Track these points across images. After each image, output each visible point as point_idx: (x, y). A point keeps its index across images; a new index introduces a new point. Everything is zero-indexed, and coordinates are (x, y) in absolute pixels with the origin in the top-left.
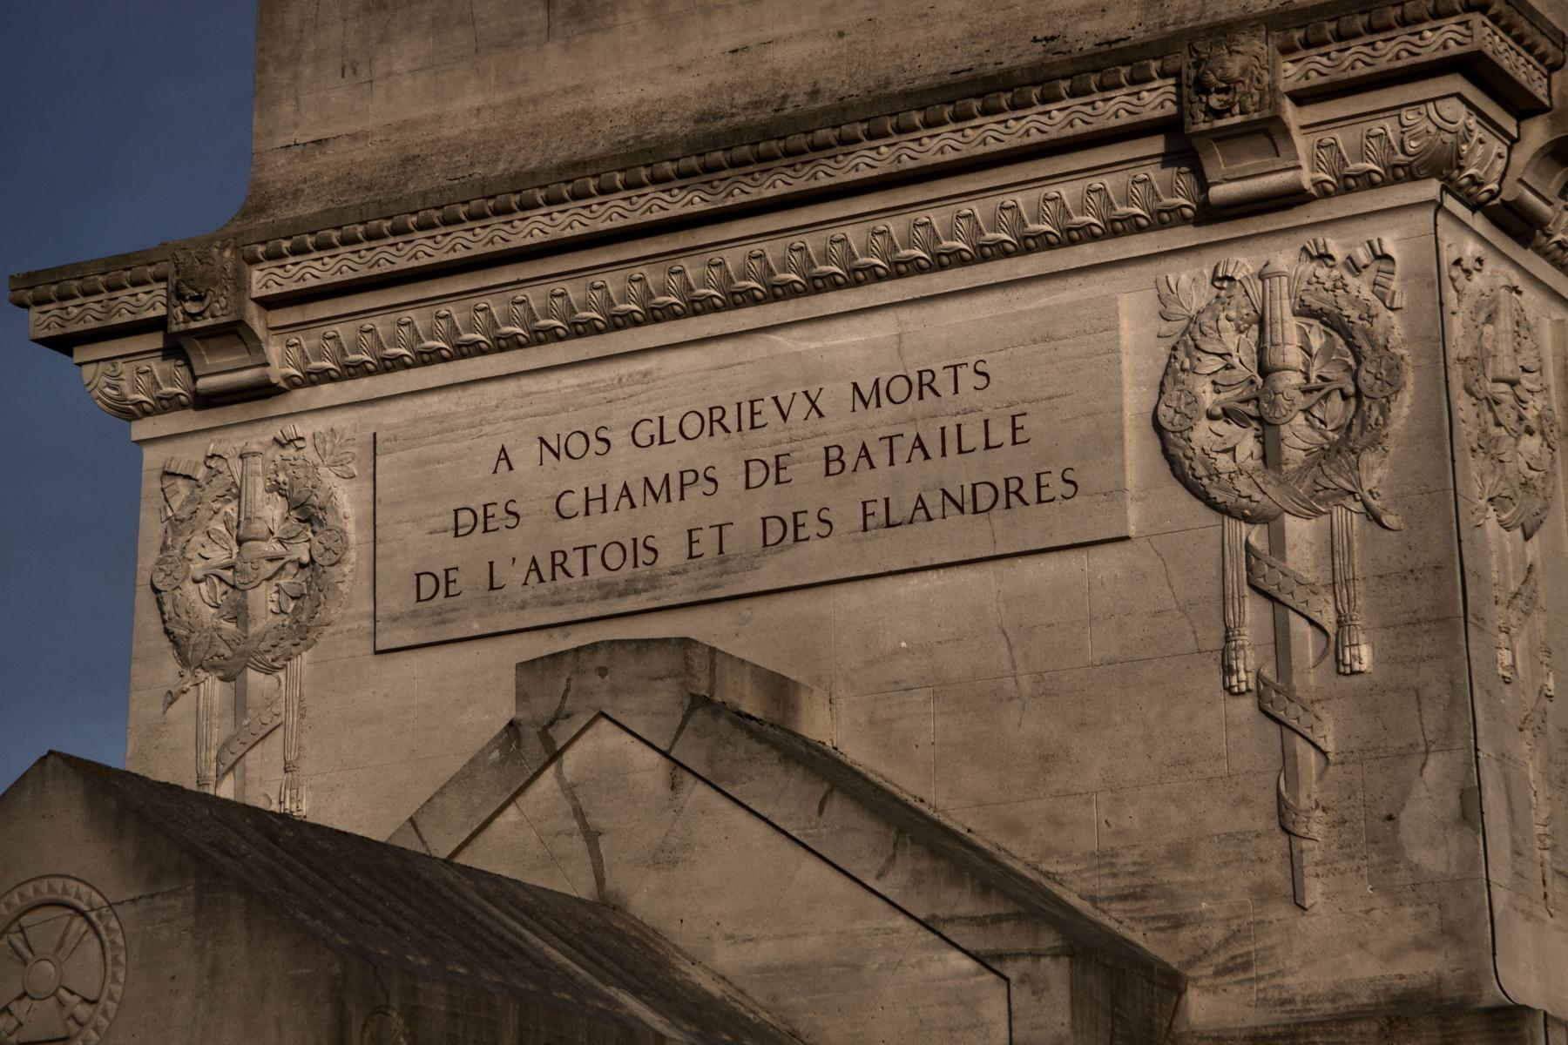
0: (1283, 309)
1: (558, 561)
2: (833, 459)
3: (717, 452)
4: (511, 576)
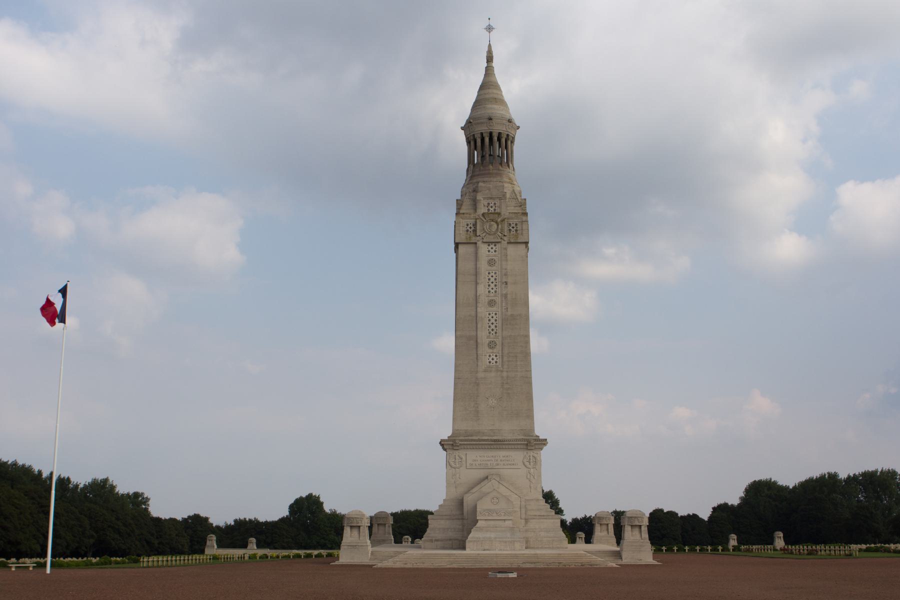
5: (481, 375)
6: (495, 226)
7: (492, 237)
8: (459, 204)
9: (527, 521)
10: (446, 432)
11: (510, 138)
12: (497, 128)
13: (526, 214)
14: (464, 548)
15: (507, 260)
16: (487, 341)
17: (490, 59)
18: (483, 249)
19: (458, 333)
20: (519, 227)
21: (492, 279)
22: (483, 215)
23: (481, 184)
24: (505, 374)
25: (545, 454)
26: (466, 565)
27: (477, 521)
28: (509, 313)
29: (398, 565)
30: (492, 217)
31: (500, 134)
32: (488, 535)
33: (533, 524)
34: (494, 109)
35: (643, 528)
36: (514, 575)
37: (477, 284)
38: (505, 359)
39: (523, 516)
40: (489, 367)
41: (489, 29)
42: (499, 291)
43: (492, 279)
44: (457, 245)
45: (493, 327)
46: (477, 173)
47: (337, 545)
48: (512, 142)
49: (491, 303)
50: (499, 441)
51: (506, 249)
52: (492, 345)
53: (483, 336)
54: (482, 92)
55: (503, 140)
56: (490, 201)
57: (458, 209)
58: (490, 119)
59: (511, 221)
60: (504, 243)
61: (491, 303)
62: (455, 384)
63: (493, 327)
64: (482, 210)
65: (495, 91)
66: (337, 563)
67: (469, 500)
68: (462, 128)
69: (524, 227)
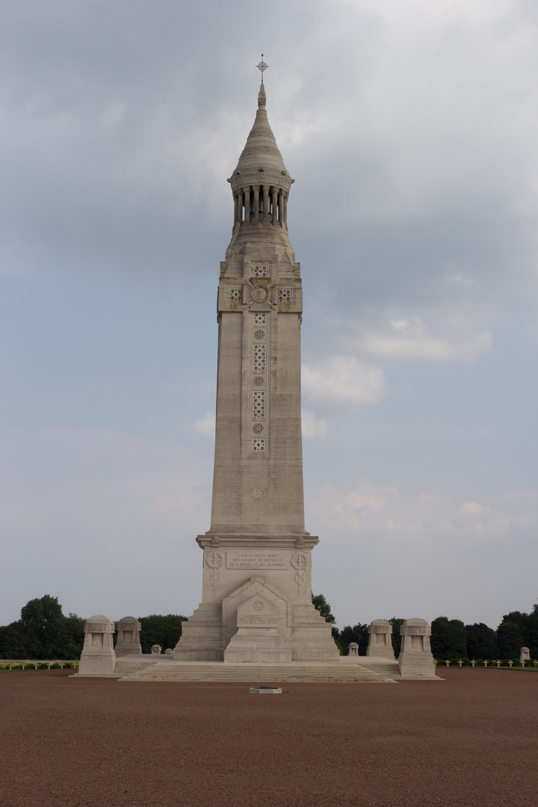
0: (300, 555)
1: (242, 564)
2: (266, 560)
3: (257, 558)
4: (239, 565)
5: (244, 462)
6: (264, 293)
7: (260, 305)
8: (224, 267)
9: (293, 629)
10: (204, 528)
11: (284, 193)
12: (268, 182)
13: (299, 280)
14: (222, 659)
15: (276, 333)
16: (253, 424)
17: (262, 102)
18: (250, 319)
19: (220, 415)
20: (291, 295)
21: (260, 354)
22: (251, 280)
23: (248, 245)
24: (272, 462)
25: (316, 553)
26: (224, 679)
27: (237, 629)
28: (279, 392)
29: (146, 678)
30: (260, 282)
31: (271, 188)
32: (249, 645)
33: (300, 633)
34: (266, 160)
35: (424, 638)
36: (279, 691)
37: (242, 358)
38: (273, 444)
39: (290, 624)
41: (262, 67)
42: (267, 367)
43: (260, 354)
44: (220, 314)
45: (259, 408)
46: (244, 232)
47: (78, 656)
48: (286, 198)
49: (258, 381)
50: (264, 538)
51: (275, 319)
52: (258, 429)
53: (249, 419)
54: (253, 139)
55: (275, 196)
56: (259, 265)
57: (223, 273)
58: (261, 171)
60: (274, 313)
61: (258, 381)
62: (215, 473)
63: (259, 408)
64: (249, 274)
65: (267, 139)
66: (75, 675)
67: (228, 605)
68: (229, 181)
69: (297, 295)
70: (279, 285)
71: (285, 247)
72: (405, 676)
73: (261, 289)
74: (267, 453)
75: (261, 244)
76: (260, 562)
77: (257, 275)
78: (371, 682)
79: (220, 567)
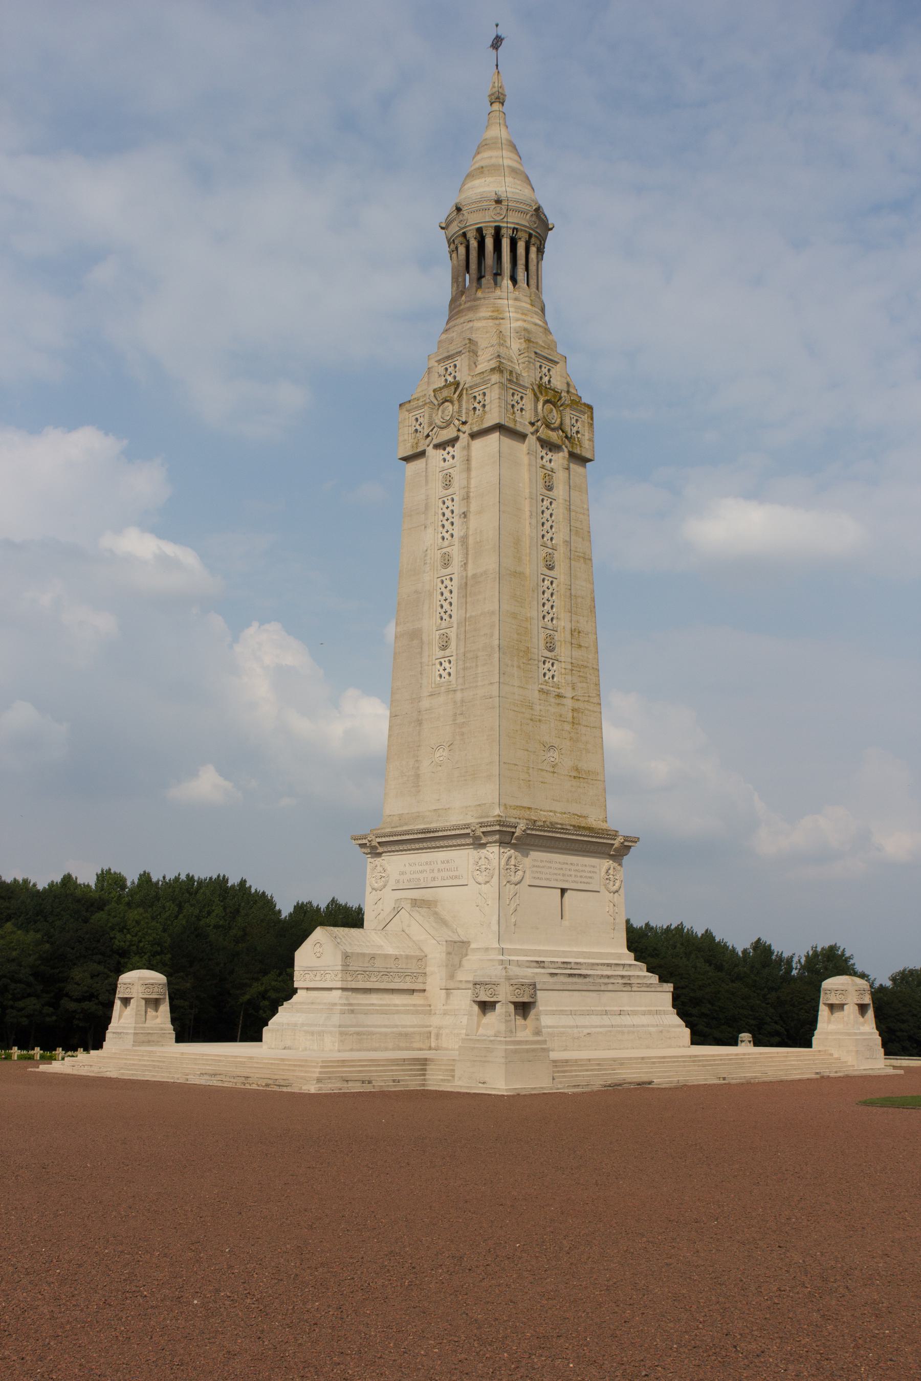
7: (445, 432)
24: (459, 695)
27: (295, 991)
40: (439, 686)
51: (468, 447)
53: (430, 625)
59: (477, 392)
60: (464, 438)
70: (471, 387)
71: (497, 322)
72: (460, 1083)
73: (447, 404)
74: (454, 682)
75: (456, 328)
76: (432, 875)
77: (446, 380)
78: (285, 1089)
79: (384, 886)
